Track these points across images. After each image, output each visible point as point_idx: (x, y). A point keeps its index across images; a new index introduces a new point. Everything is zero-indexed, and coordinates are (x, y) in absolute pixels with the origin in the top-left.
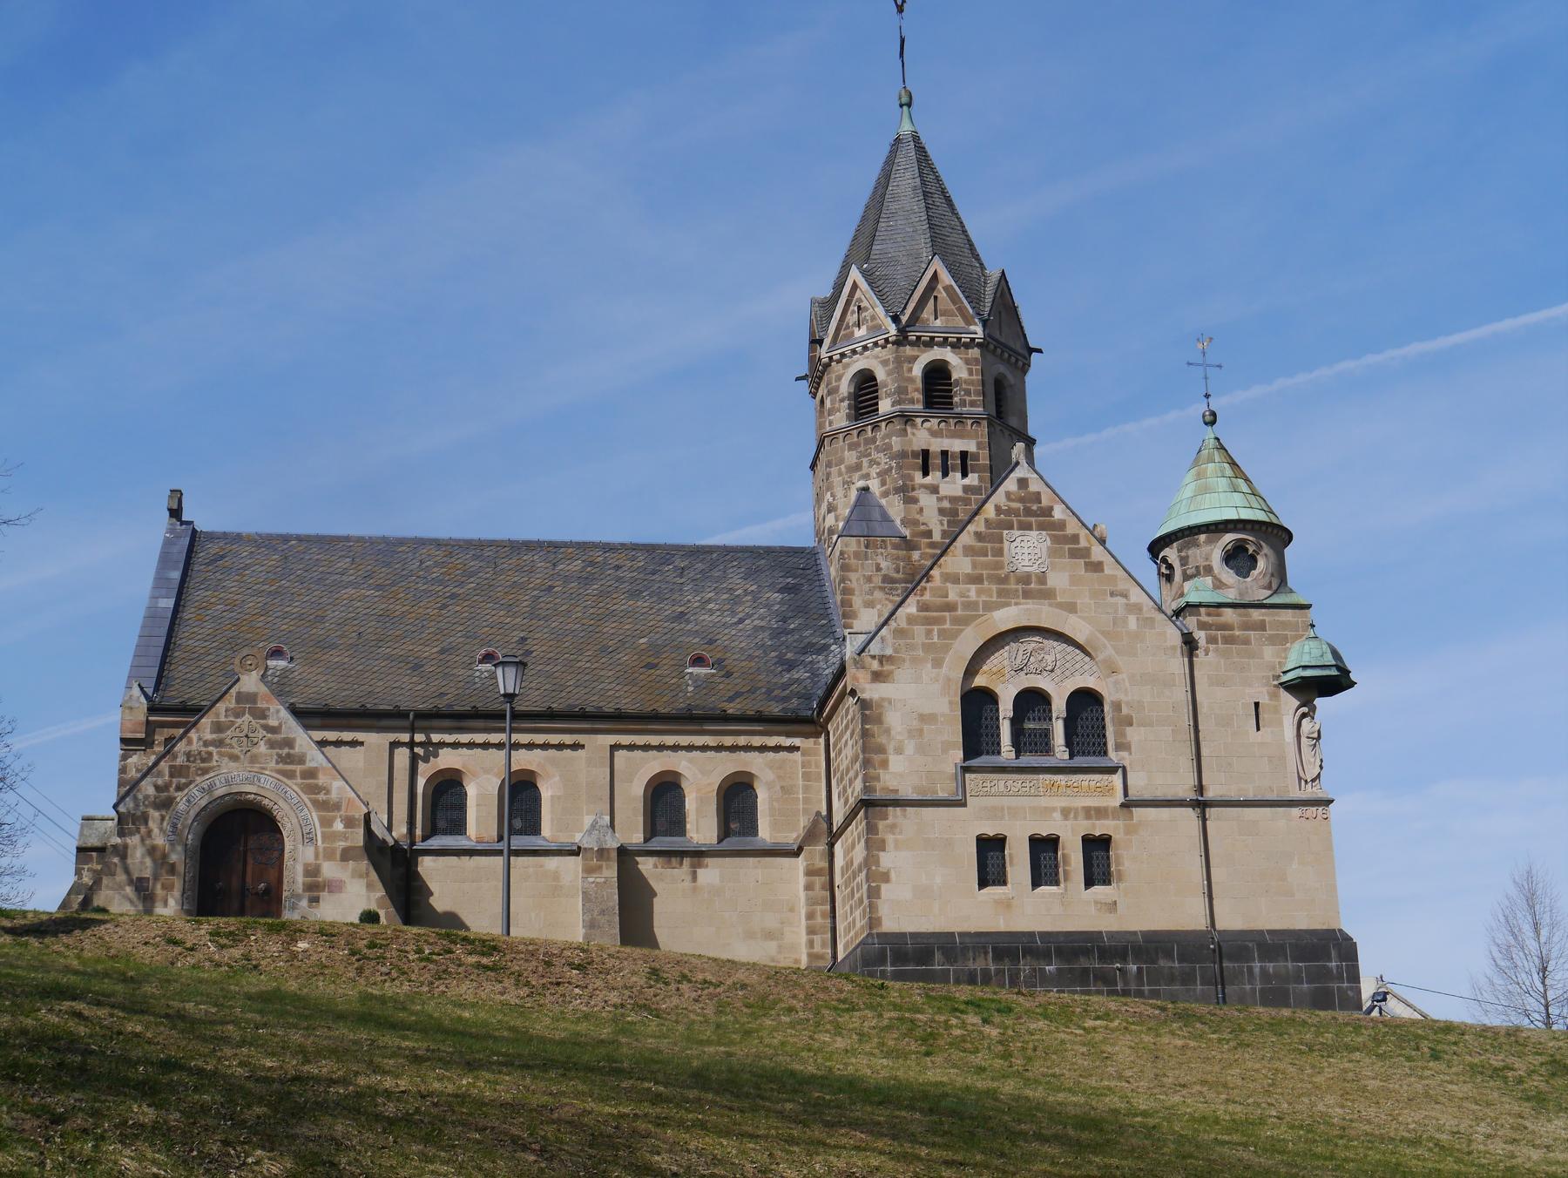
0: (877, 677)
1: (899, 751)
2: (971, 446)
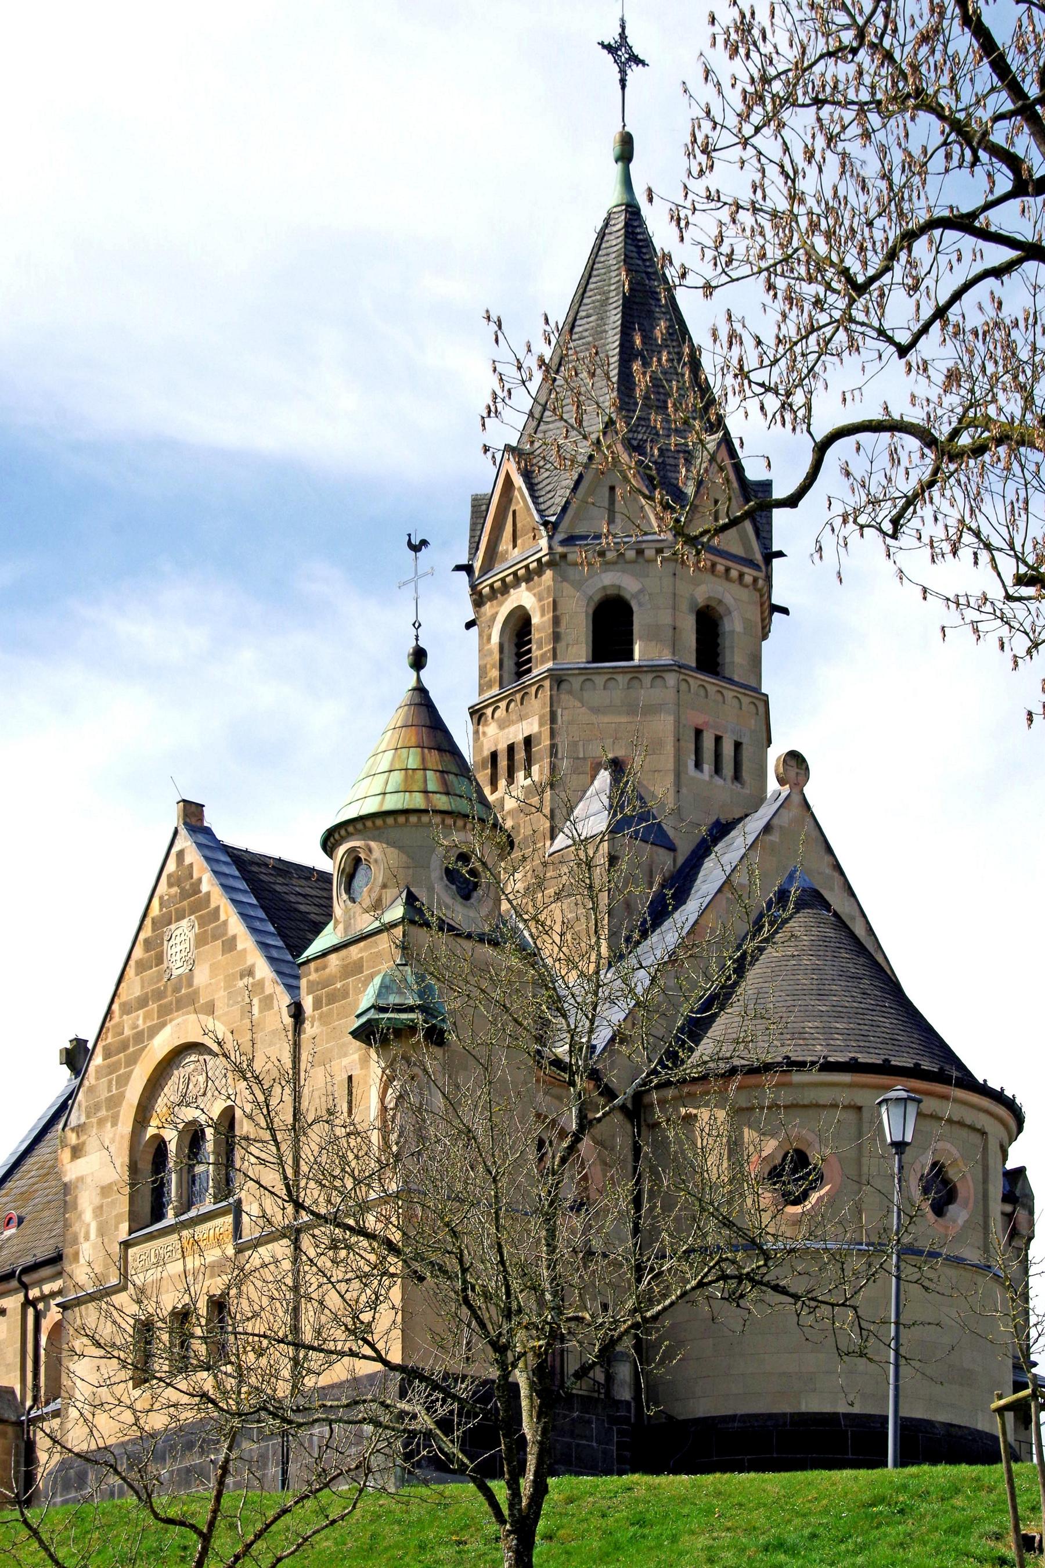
0: (77, 1152)
1: (87, 1238)
2: (531, 726)
